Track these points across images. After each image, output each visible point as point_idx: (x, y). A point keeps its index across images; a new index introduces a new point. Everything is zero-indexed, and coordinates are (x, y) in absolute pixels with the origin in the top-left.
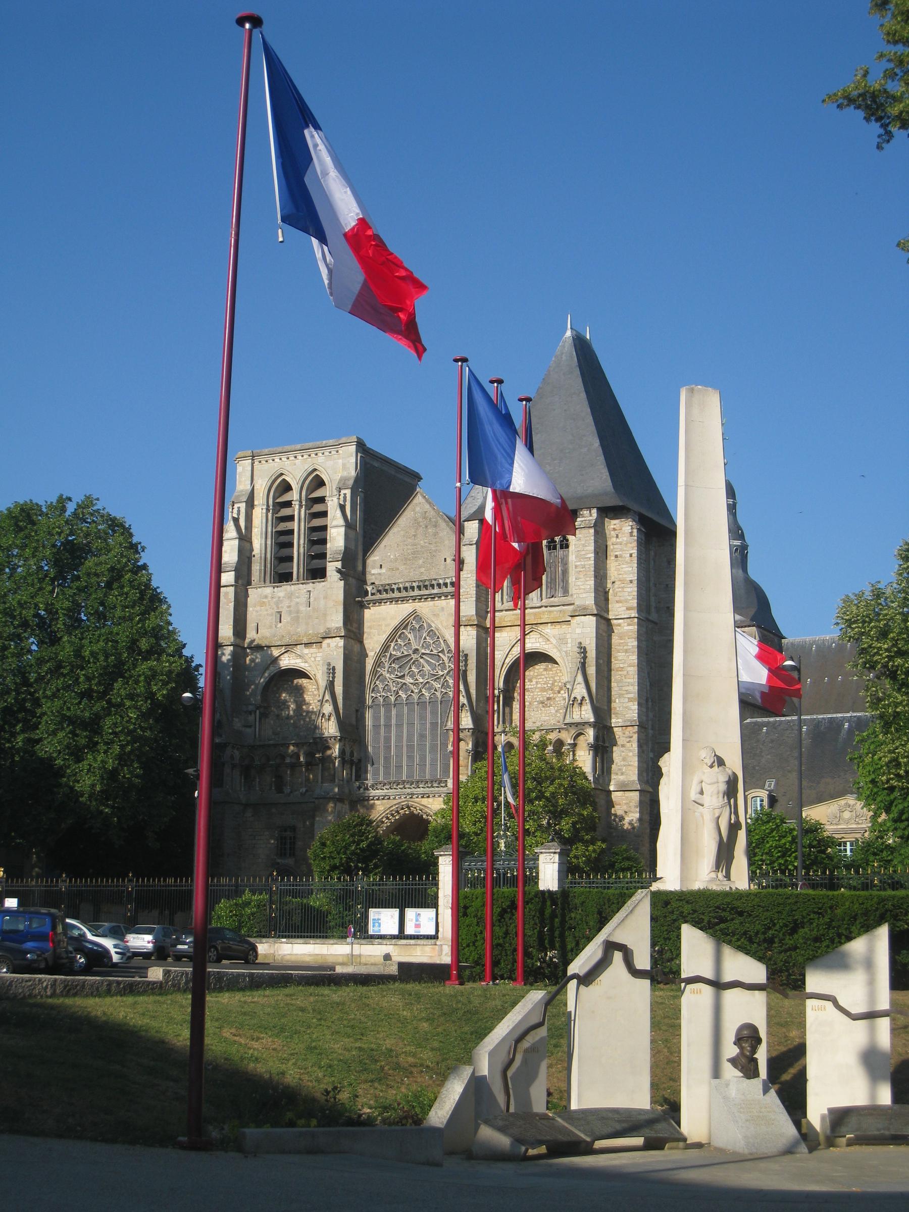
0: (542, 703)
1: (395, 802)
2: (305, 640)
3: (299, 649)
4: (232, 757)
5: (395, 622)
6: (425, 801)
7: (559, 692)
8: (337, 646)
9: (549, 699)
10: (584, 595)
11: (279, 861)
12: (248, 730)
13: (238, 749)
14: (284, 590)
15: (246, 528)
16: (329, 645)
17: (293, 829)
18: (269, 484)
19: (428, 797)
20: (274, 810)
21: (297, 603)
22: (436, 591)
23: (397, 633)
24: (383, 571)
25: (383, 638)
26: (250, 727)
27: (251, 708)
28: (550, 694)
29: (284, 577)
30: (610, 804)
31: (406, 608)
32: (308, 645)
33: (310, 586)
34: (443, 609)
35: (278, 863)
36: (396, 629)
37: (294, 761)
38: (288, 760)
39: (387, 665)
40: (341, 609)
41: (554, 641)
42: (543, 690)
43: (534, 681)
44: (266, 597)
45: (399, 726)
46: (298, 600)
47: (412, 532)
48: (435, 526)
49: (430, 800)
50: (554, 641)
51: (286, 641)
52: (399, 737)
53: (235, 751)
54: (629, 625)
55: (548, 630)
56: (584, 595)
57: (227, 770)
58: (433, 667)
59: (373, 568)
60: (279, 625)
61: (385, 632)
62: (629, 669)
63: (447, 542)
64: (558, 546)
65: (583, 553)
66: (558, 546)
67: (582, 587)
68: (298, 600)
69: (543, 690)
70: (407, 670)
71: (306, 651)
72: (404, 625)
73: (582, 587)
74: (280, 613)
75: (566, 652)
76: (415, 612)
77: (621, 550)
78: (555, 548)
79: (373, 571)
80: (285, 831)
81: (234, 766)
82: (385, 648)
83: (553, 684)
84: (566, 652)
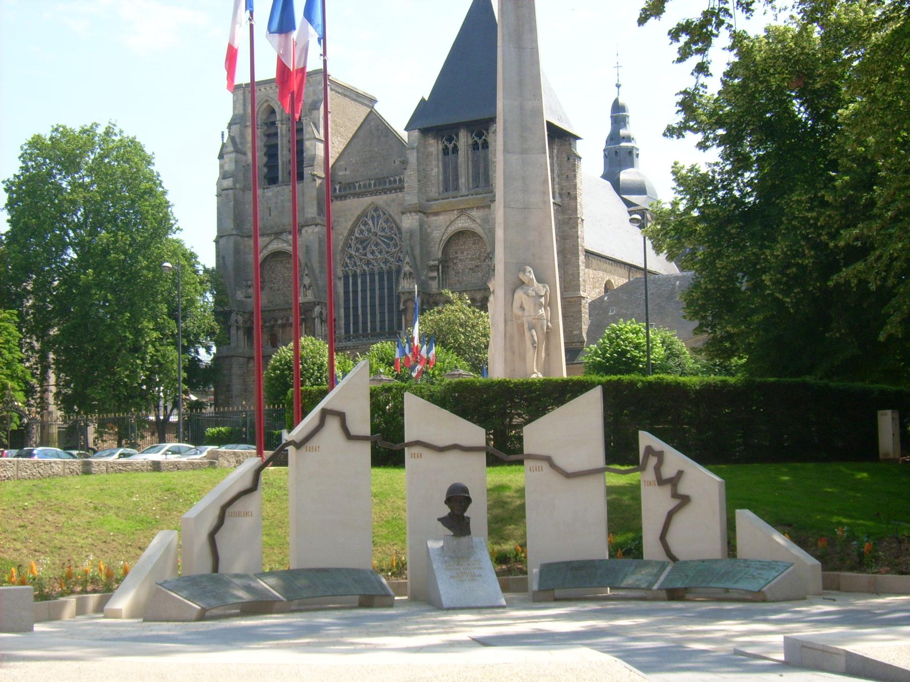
4: (237, 321)
5: (358, 212)
8: (313, 232)
9: (477, 266)
12: (248, 300)
16: (306, 231)
21: (283, 201)
22: (388, 186)
23: (361, 219)
25: (350, 224)
29: (272, 180)
31: (367, 200)
34: (393, 200)
36: (358, 219)
37: (284, 322)
38: (280, 322)
39: (353, 245)
40: (315, 202)
41: (479, 221)
42: (472, 259)
45: (364, 291)
50: (479, 221)
51: (275, 229)
55: (475, 213)
57: (233, 331)
58: (388, 246)
69: (472, 259)
70: (368, 249)
72: (364, 214)
76: (372, 203)
78: (478, 149)
81: (238, 328)
82: (351, 232)
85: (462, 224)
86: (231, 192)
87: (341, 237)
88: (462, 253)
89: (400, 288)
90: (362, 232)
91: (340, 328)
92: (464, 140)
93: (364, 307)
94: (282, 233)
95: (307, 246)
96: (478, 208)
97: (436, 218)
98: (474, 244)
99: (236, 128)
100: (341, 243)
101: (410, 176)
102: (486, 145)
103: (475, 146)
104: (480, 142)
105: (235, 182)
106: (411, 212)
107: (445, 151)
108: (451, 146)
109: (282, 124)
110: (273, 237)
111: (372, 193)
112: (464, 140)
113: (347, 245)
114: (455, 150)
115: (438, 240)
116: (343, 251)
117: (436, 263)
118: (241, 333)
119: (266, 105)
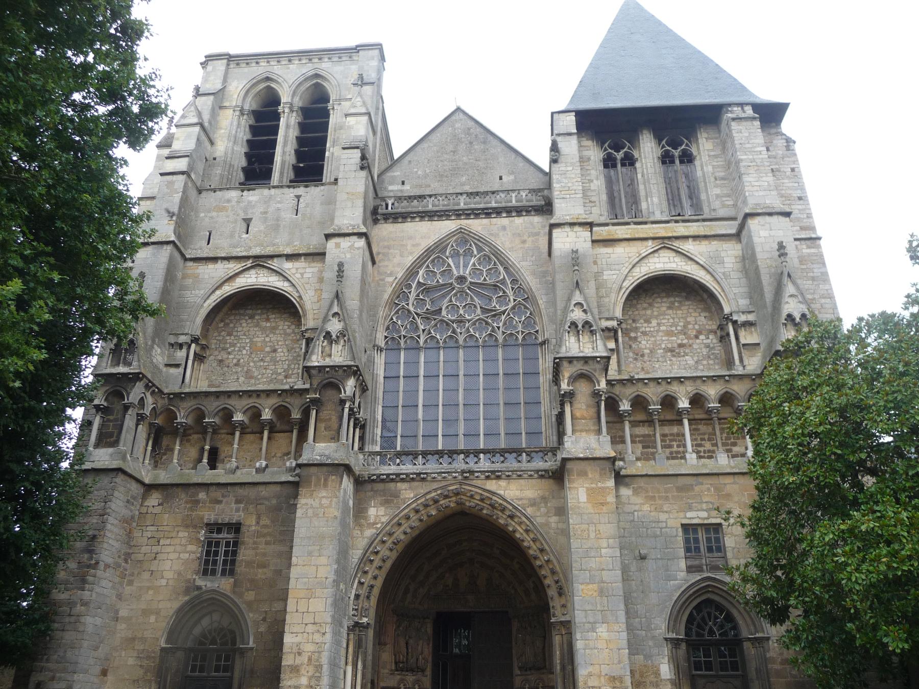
0: (671, 350)
1: (435, 485)
2: (288, 251)
3: (275, 264)
6: (491, 485)
7: (697, 337)
10: (761, 193)
11: (200, 582)
12: (173, 371)
13: (153, 393)
14: (255, 196)
15: (210, 123)
16: (338, 245)
17: (236, 528)
18: (248, 86)
19: (498, 478)
20: (202, 495)
21: (279, 209)
23: (435, 253)
24: (407, 187)
25: (409, 260)
26: (177, 366)
27: (182, 339)
28: (682, 339)
30: (333, 617)
31: (448, 226)
32: (290, 257)
33: (301, 191)
34: (504, 228)
35: (199, 588)
36: (429, 252)
43: (654, 322)
44: (229, 201)
46: (279, 205)
47: (451, 148)
48: (484, 143)
49: (503, 483)
51: (257, 251)
52: (431, 391)
53: (148, 394)
54: (809, 247)
55: (689, 247)
56: (761, 193)
57: (129, 421)
59: (391, 184)
60: (245, 236)
61: (411, 253)
62: (823, 301)
63: (501, 159)
64: (677, 161)
65: (748, 146)
66: (677, 161)
67: (756, 184)
68: (279, 205)
69: (669, 333)
71: (288, 266)
73: (756, 184)
74: (248, 222)
75: (724, 274)
76: (460, 231)
77: (777, 164)
78: (672, 162)
79: (390, 188)
80: (219, 531)
81: (140, 418)
82: (412, 273)
83: (685, 327)
84: (724, 274)
85: (665, 263)
86: (182, 178)
87: (391, 279)
88: (648, 321)
89: (563, 349)
90: (429, 272)
91: (373, 442)
92: (648, 149)
93: (430, 406)
94: (272, 257)
95: (341, 265)
96: (695, 237)
97: (609, 250)
98: (669, 308)
99: (206, 103)
100: (390, 290)
101: (564, 173)
102: (687, 158)
103: (666, 159)
104: (676, 153)
105: (191, 166)
106: (572, 224)
107: (609, 162)
108: (619, 156)
109: (292, 111)
110: (249, 263)
111: (459, 214)
112: (648, 149)
113: (401, 293)
114: (629, 161)
115: (616, 287)
116: (392, 303)
117: (614, 324)
118: (142, 430)
119: (262, 86)
